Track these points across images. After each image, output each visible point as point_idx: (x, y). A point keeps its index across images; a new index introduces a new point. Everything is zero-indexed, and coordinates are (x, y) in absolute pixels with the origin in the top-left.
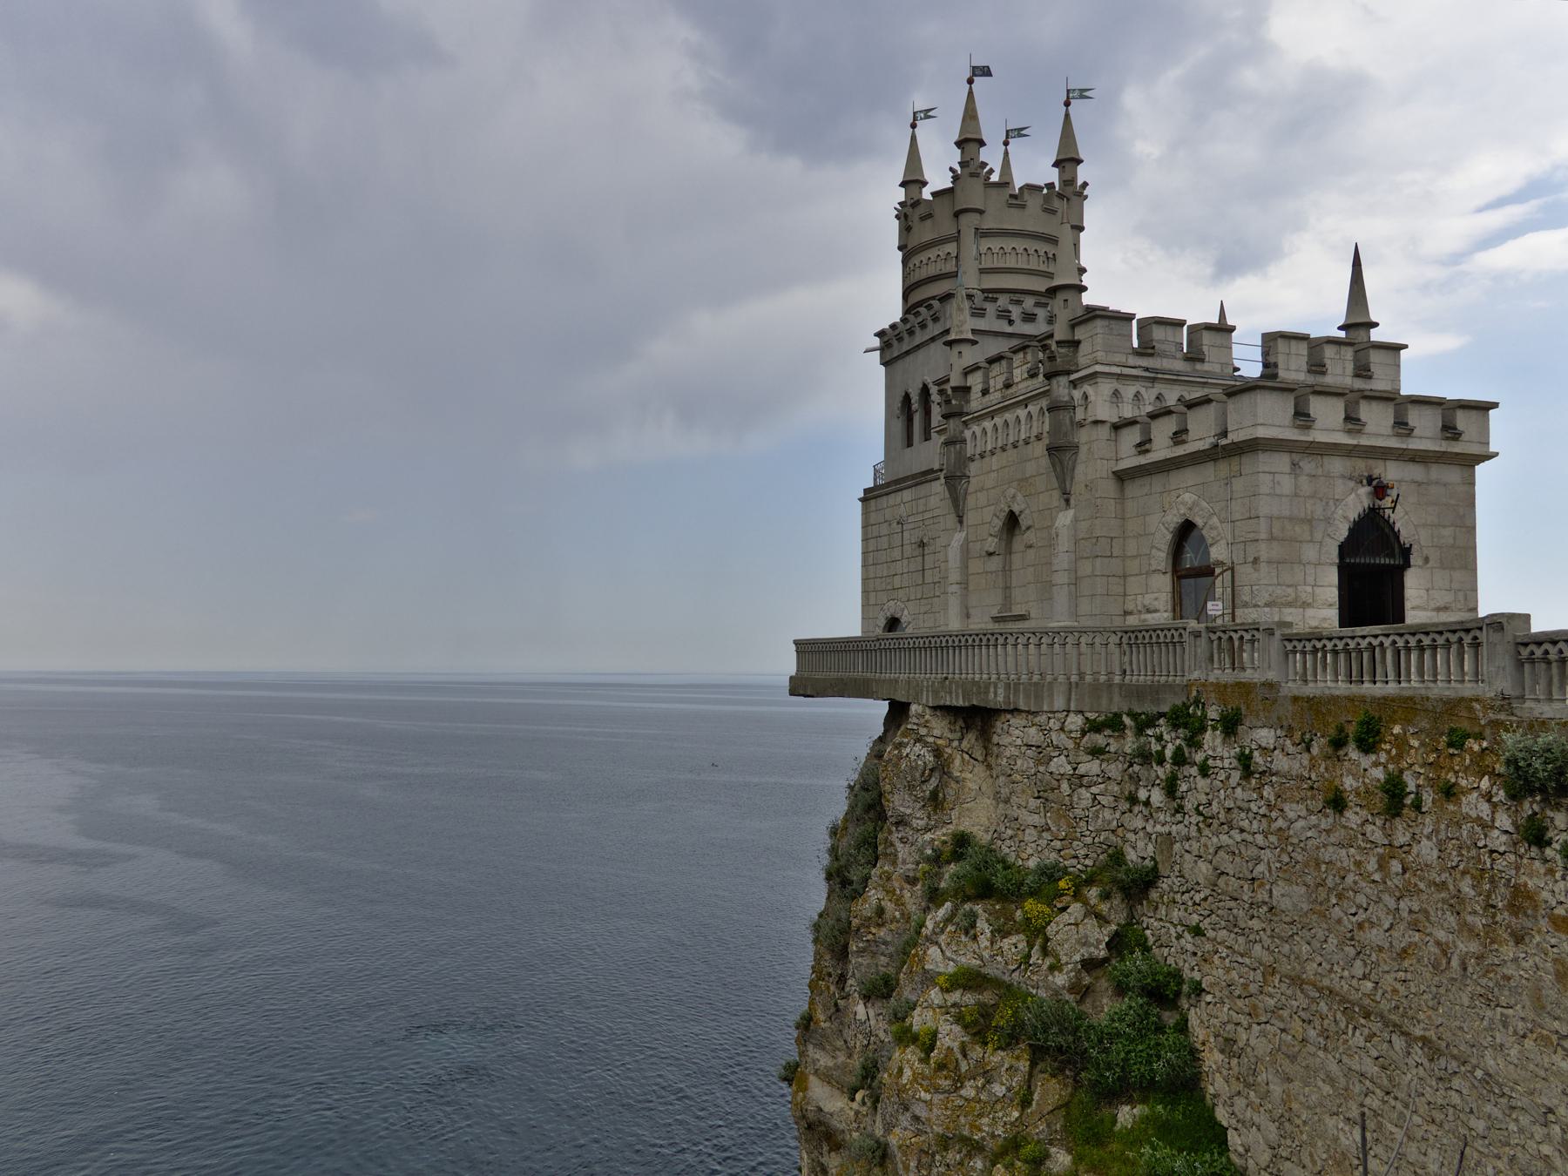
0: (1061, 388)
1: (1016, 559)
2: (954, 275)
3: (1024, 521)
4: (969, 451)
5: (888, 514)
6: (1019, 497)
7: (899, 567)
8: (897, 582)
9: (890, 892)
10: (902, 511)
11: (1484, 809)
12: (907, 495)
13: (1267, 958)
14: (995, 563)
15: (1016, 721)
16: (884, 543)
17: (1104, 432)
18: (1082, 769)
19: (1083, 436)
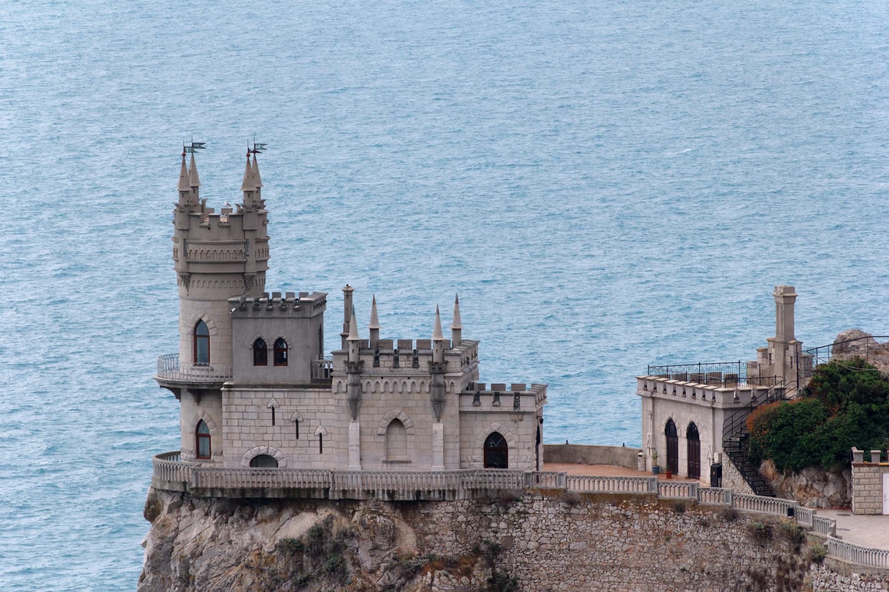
0: (440, 379)
1: (392, 438)
2: (245, 263)
3: (407, 423)
4: (364, 389)
5: (255, 401)
6: (403, 413)
7: (270, 430)
8: (266, 437)
9: (364, 578)
10: (273, 402)
11: (657, 517)
12: (277, 395)
13: (567, 563)
14: (382, 439)
15: (444, 504)
16: (255, 416)
17: (456, 398)
18: (469, 519)
19: (449, 398)
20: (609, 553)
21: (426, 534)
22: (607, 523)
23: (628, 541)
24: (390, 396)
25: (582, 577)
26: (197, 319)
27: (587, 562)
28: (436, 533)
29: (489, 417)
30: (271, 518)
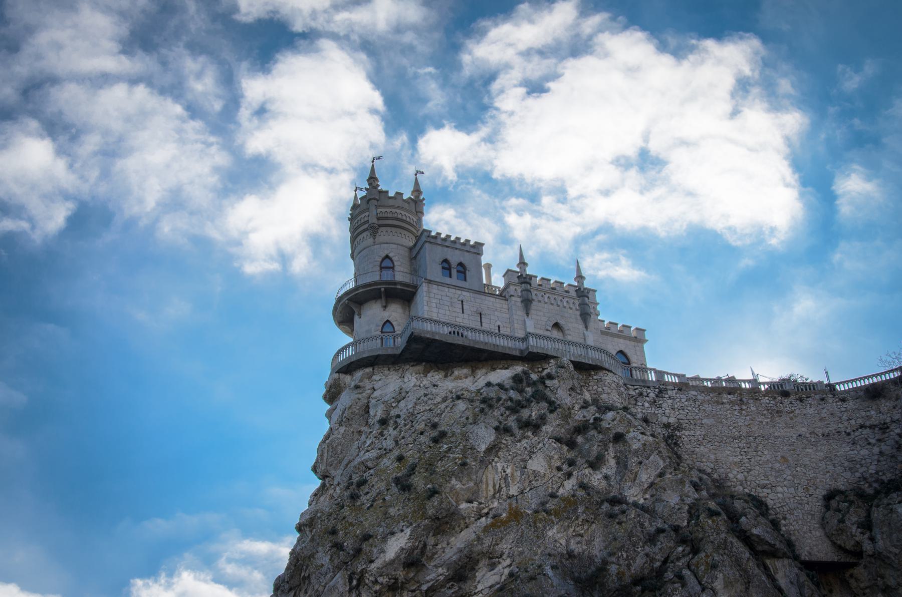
8: (458, 319)
12: (464, 293)
13: (703, 433)
15: (610, 374)
16: (449, 304)
20: (734, 427)
21: (601, 394)
22: (728, 406)
23: (748, 418)
24: (552, 307)
25: (717, 444)
26: (384, 255)
27: (718, 433)
28: (608, 394)
29: (616, 339)
30: (466, 377)
